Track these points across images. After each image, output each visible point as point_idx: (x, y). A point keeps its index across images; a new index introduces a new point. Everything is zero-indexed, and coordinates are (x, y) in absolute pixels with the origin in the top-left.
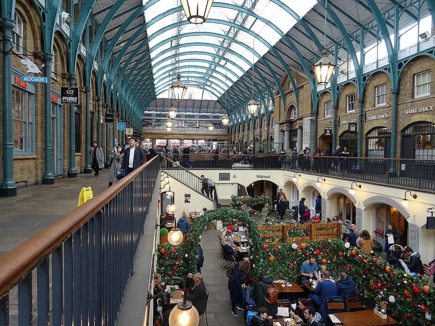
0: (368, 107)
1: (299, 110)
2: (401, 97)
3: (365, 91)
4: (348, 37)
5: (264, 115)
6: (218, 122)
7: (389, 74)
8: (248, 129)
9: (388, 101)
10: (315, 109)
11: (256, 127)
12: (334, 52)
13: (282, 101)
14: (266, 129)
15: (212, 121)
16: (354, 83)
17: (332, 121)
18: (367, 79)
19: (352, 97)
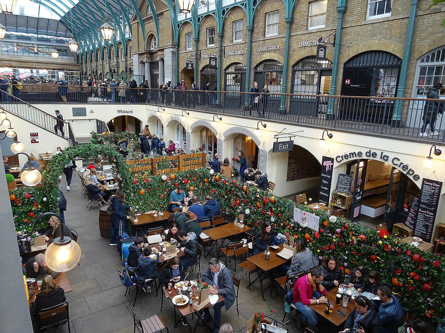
0: (227, 43)
1: (160, 40)
2: (255, 35)
8: (103, 59)
10: (176, 41)
11: (112, 57)
13: (140, 28)
15: (56, 46)
17: (194, 54)
19: (212, 31)
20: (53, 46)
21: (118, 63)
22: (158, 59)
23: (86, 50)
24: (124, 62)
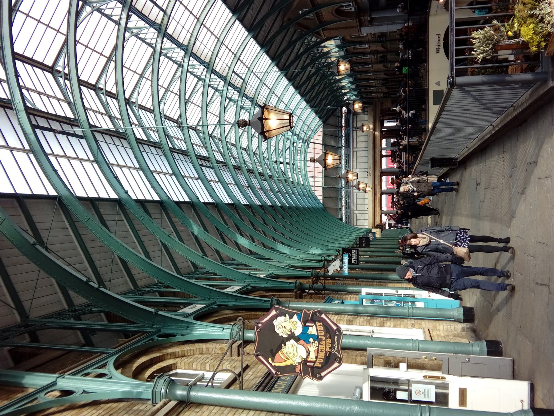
5: (346, 50)
8: (367, 72)
21: (372, 53)
24: (371, 45)
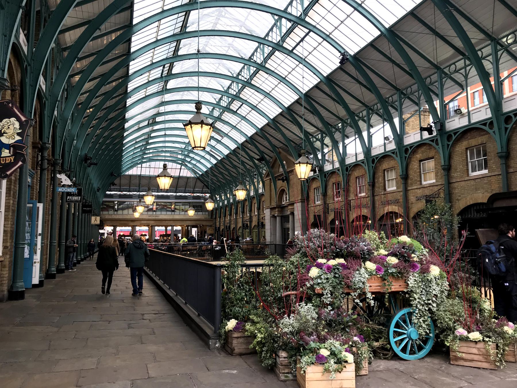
2: (376, 189)
3: (450, 157)
4: (385, 103)
5: (254, 197)
6: (198, 204)
7: (437, 147)
8: (236, 213)
9: (367, 191)
10: (305, 196)
11: (245, 211)
12: (365, 118)
14: (256, 213)
15: (192, 202)
16: (363, 165)
17: (322, 207)
18: (376, 161)
19: (338, 185)
20: (189, 203)
21: (251, 217)
22: (289, 213)
23: (221, 204)
24: (257, 217)
